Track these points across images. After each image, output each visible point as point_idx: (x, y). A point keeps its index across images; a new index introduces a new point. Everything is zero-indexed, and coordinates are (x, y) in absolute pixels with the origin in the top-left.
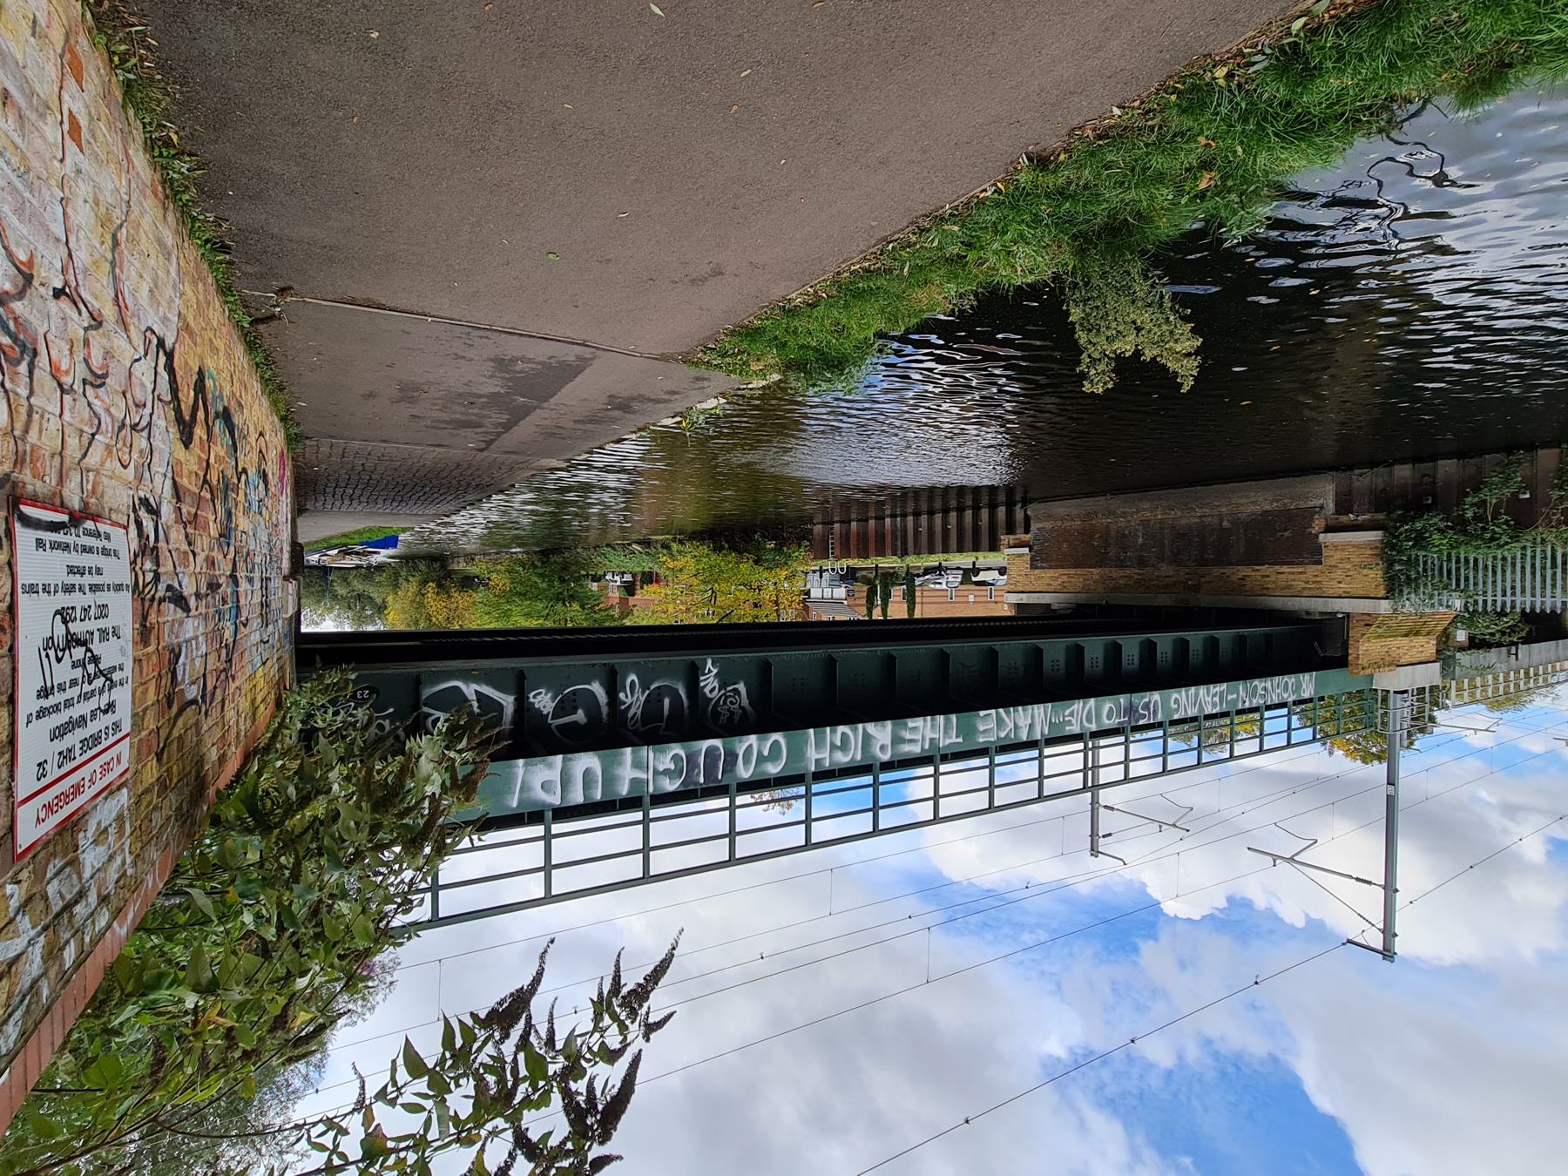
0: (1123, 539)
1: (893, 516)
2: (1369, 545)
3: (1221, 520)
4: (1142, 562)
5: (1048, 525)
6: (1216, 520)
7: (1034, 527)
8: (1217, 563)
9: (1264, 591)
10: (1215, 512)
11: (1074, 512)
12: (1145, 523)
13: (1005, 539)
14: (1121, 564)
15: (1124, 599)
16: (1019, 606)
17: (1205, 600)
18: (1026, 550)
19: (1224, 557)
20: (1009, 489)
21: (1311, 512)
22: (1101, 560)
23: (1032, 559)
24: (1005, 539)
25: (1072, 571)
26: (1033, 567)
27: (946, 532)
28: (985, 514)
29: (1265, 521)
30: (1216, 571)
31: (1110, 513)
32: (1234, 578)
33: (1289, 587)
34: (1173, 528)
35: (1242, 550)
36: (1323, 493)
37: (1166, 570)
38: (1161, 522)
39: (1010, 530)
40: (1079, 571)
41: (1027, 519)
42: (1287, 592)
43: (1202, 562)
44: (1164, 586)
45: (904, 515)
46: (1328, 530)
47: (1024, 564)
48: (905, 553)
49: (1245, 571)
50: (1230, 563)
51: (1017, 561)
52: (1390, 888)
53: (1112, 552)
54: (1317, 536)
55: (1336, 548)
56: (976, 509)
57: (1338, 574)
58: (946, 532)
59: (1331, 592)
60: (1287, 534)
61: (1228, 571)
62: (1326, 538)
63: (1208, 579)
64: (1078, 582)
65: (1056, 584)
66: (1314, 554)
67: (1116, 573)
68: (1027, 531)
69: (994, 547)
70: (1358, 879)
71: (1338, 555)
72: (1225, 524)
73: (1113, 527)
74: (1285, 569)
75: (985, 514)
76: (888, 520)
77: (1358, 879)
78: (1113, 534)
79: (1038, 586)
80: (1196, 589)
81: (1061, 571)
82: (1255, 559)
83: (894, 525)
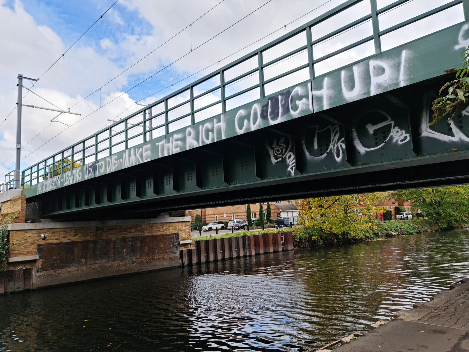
0: (133, 251)
1: (250, 256)
2: (16, 255)
3: (86, 262)
4: (124, 240)
5: (171, 255)
6: (89, 262)
7: (178, 254)
8: (89, 242)
9: (65, 230)
10: (88, 266)
11: (158, 263)
12: (123, 259)
13: (193, 247)
14: (134, 238)
15: (132, 222)
16: (184, 215)
17: (93, 224)
18: (182, 242)
19: (85, 245)
20: (191, 273)
21: (42, 269)
22: (144, 240)
23: (178, 238)
24: (193, 247)
25: (158, 233)
26: (178, 235)
27: (223, 249)
28: (203, 259)
29: (64, 263)
30: (88, 238)
31: (140, 263)
32: (80, 235)
33: (54, 233)
34: (109, 258)
35: (76, 248)
36: (37, 278)
37: (112, 237)
39: (190, 252)
40: (155, 234)
41: (181, 257)
42: (54, 231)
43: (95, 242)
44: (113, 229)
45: (245, 256)
46: (35, 261)
47: (183, 235)
48: (244, 237)
50: (82, 242)
51: (185, 237)
52: (19, 104)
53: (139, 244)
54: (40, 258)
55: (31, 253)
56: (208, 262)
57: (30, 240)
58: (223, 249)
59: (34, 232)
60: (54, 258)
61: (83, 239)
62: (37, 257)
63: (92, 234)
64: (155, 229)
65: (166, 227)
66: (41, 249)
67: (136, 234)
68: (181, 252)
69: (198, 243)
70: (33, 107)
71: (30, 249)
72: (83, 261)
73: (138, 256)
74: (55, 241)
75: (203, 259)
76: (253, 253)
77: (33, 107)
78: (138, 253)
79: (175, 226)
80: (98, 229)
81: (163, 233)
82: (70, 245)
83: (250, 251)
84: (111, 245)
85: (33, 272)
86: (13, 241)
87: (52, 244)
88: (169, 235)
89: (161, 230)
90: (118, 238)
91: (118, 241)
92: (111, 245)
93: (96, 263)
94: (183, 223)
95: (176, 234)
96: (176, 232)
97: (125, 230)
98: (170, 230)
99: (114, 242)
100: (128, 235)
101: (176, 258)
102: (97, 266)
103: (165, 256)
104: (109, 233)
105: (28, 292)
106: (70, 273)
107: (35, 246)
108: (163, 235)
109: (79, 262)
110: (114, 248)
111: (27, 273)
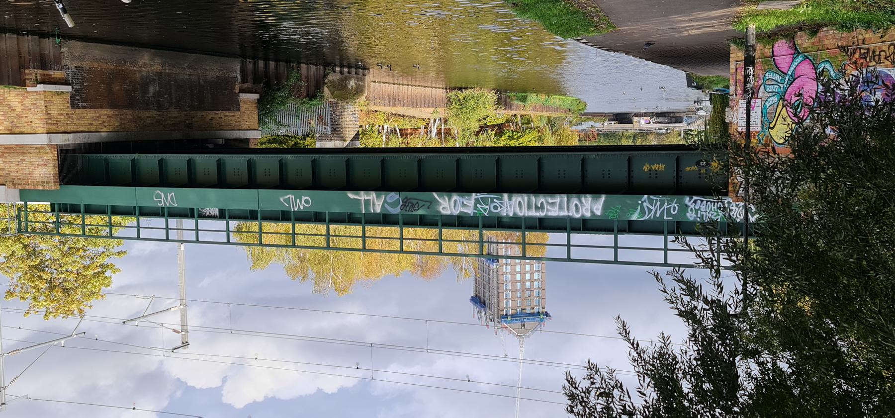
0: (145, 84)
4: (160, 107)
5: (86, 64)
13: (32, 73)
14: (146, 106)
18: (68, 89)
22: (131, 104)
23: (73, 98)
24: (32, 73)
25: (109, 112)
26: (74, 106)
30: (199, 114)
33: (230, 124)
34: (176, 81)
36: (236, 69)
37: (174, 113)
38: (169, 75)
39: (43, 63)
40: (116, 112)
43: (193, 108)
46: (242, 91)
49: (211, 114)
51: (57, 100)
55: (245, 102)
57: (245, 117)
59: (244, 127)
62: (243, 96)
67: (144, 114)
74: (227, 113)
84: (174, 100)
85: (239, 77)
86: (256, 117)
87: (229, 110)
88: (91, 108)
89: (105, 118)
90: (167, 109)
91: (167, 105)
92: (174, 100)
93: (190, 75)
94: (63, 129)
95: (78, 107)
96: (78, 111)
97: (158, 122)
98: (89, 114)
99: (171, 104)
100: (153, 113)
101: (74, 58)
102: (188, 71)
103: (96, 65)
104: (178, 119)
105: (243, 56)
106: (212, 69)
107: (242, 110)
108: (101, 107)
109: (206, 81)
110: (170, 95)
111: (244, 80)
